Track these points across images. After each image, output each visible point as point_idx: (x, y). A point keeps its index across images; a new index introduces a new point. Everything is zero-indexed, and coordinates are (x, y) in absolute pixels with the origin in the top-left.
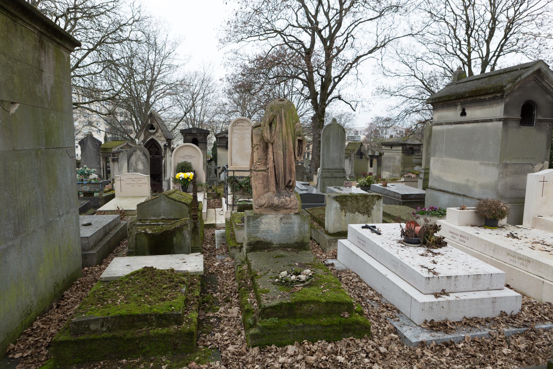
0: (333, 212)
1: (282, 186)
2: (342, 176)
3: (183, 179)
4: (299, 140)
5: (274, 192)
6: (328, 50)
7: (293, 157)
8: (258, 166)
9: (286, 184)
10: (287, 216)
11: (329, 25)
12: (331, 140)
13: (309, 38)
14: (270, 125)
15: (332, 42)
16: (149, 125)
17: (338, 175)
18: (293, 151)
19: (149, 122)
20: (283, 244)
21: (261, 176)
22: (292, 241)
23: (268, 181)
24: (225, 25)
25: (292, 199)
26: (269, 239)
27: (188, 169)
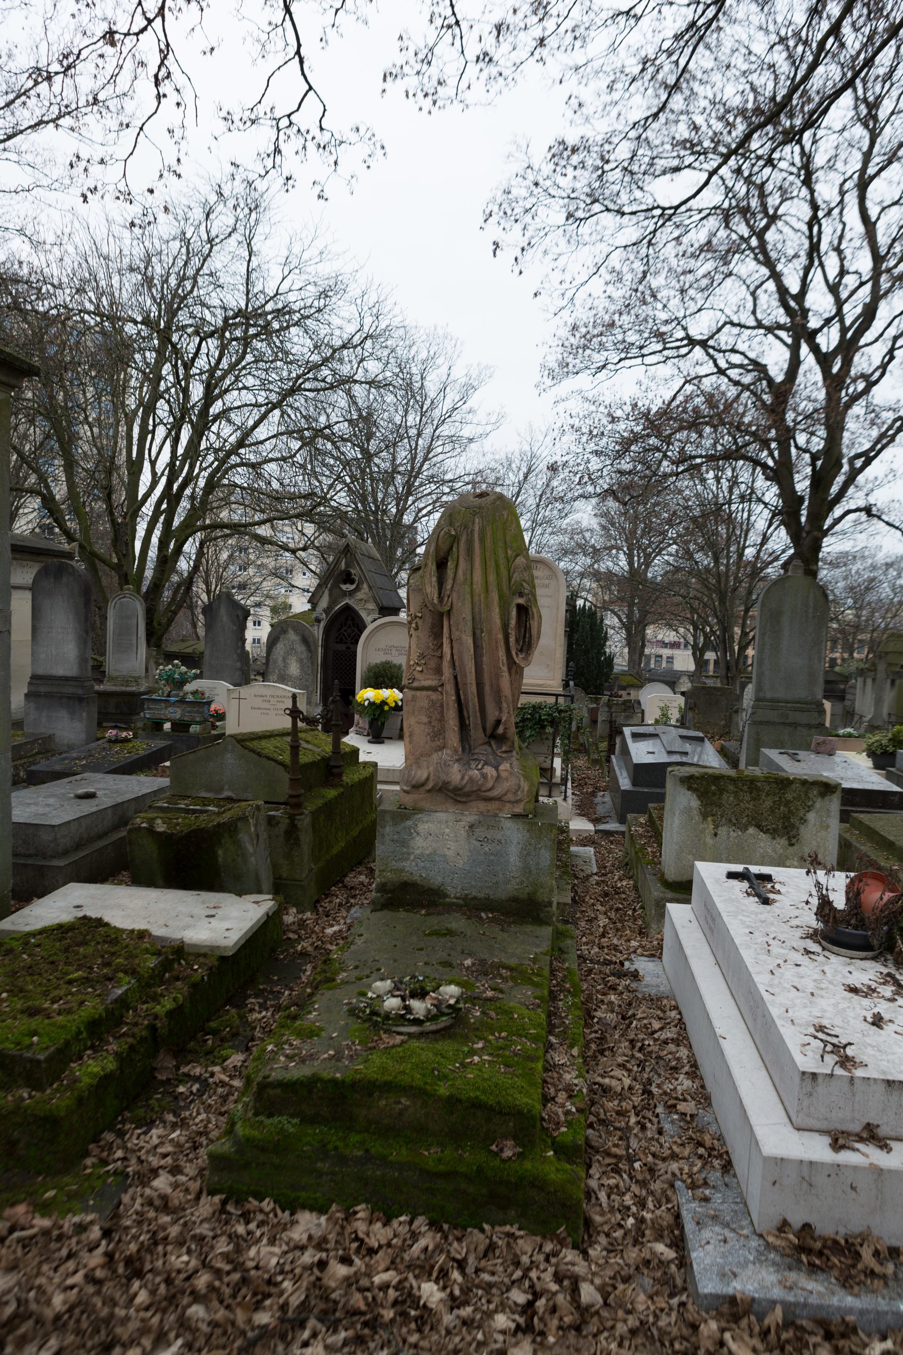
0: (677, 821)
1: (477, 734)
3: (372, 704)
4: (520, 607)
5: (456, 751)
6: (834, 383)
7: (502, 654)
8: (418, 676)
9: (489, 731)
10: (490, 821)
11: (839, 313)
13: (785, 354)
14: (441, 565)
15: (847, 363)
16: (342, 572)
17: (803, 718)
18: (500, 636)
19: (343, 565)
20: (475, 898)
21: (425, 703)
22: (502, 893)
23: (442, 719)
24: (564, 332)
25: (504, 775)
26: (436, 879)
27: (391, 679)
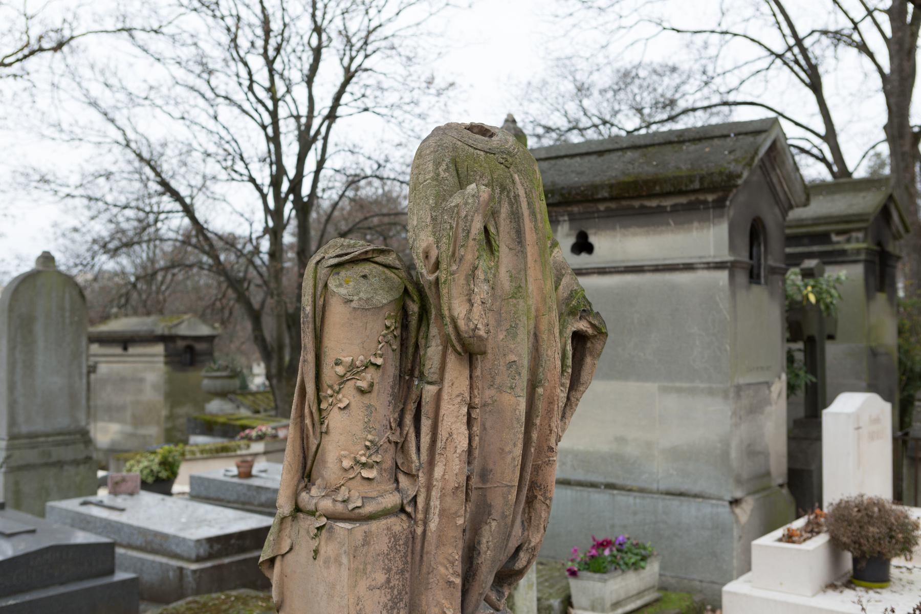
2: (81, 456)
12: (39, 328)
